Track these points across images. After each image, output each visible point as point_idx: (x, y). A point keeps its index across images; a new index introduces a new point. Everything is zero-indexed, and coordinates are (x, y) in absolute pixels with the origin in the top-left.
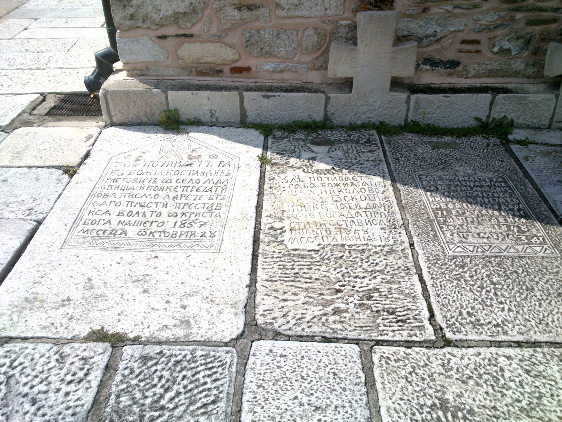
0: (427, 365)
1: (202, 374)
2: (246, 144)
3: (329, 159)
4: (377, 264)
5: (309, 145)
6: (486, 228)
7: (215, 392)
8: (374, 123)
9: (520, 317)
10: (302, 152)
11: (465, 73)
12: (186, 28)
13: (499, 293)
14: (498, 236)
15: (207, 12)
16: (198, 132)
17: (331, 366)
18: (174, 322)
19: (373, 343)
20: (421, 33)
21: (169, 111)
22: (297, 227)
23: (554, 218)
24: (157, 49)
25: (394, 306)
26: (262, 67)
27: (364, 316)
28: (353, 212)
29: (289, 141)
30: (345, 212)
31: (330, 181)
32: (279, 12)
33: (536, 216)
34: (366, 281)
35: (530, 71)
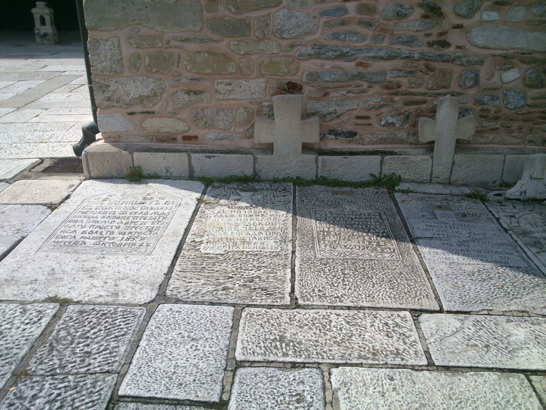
0: (278, 318)
1: (119, 320)
2: (190, 191)
3: (250, 200)
4: (264, 262)
6: (354, 243)
7: (125, 330)
8: (292, 178)
9: (355, 293)
10: (232, 195)
11: (361, 141)
12: (149, 107)
13: (346, 280)
14: (360, 247)
15: (165, 96)
16: (155, 183)
18: (107, 293)
19: (245, 306)
20: (324, 111)
21: (135, 168)
22: (212, 241)
23: (408, 238)
24: (127, 122)
25: (267, 286)
26: (207, 136)
27: (244, 292)
28: (257, 232)
29: (224, 189)
30: (251, 232)
32: (218, 96)
33: (395, 236)
34: (253, 272)
35: (412, 139)
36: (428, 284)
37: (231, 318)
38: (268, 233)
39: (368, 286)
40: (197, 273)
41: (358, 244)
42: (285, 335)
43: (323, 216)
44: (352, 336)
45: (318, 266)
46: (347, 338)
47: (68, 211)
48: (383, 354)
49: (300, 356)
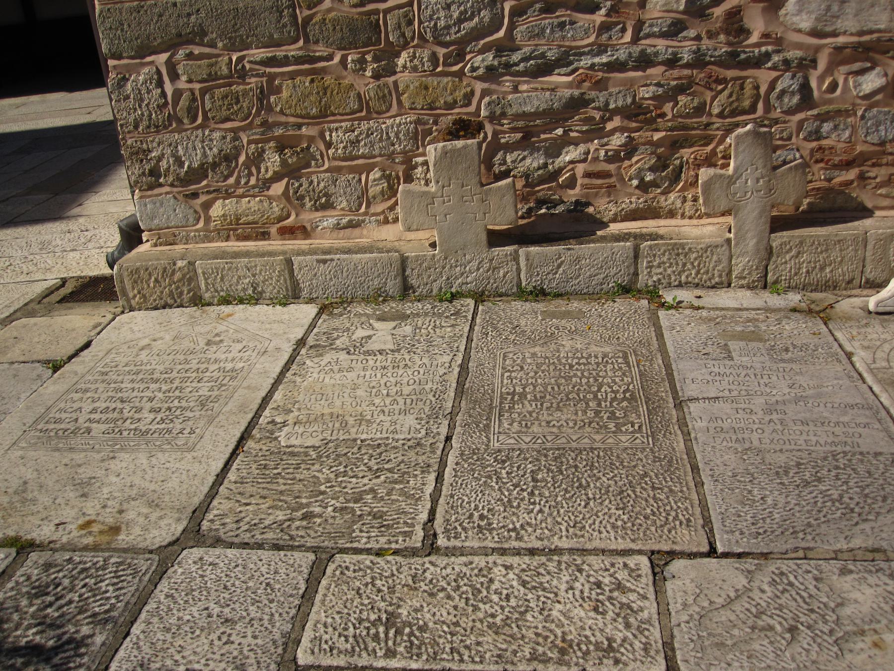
0: (393, 575)
1: (107, 582)
4: (389, 461)
5: (371, 321)
7: (113, 601)
9: (549, 520)
13: (537, 492)
14: (575, 424)
17: (268, 576)
25: (385, 509)
30: (377, 401)
31: (378, 363)
34: (366, 480)
36: (695, 496)
37: (306, 576)
38: (408, 401)
39: (576, 505)
40: (264, 485)
41: (574, 417)
42: (400, 611)
43: (519, 361)
44: (526, 611)
45: (488, 466)
46: (516, 615)
47: (79, 372)
48: (580, 649)
49: (417, 656)
